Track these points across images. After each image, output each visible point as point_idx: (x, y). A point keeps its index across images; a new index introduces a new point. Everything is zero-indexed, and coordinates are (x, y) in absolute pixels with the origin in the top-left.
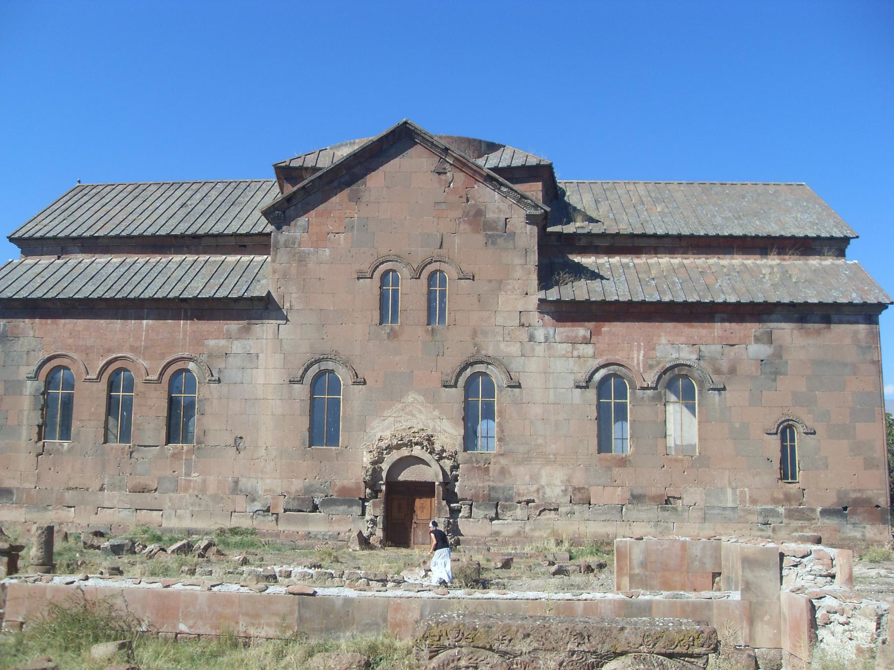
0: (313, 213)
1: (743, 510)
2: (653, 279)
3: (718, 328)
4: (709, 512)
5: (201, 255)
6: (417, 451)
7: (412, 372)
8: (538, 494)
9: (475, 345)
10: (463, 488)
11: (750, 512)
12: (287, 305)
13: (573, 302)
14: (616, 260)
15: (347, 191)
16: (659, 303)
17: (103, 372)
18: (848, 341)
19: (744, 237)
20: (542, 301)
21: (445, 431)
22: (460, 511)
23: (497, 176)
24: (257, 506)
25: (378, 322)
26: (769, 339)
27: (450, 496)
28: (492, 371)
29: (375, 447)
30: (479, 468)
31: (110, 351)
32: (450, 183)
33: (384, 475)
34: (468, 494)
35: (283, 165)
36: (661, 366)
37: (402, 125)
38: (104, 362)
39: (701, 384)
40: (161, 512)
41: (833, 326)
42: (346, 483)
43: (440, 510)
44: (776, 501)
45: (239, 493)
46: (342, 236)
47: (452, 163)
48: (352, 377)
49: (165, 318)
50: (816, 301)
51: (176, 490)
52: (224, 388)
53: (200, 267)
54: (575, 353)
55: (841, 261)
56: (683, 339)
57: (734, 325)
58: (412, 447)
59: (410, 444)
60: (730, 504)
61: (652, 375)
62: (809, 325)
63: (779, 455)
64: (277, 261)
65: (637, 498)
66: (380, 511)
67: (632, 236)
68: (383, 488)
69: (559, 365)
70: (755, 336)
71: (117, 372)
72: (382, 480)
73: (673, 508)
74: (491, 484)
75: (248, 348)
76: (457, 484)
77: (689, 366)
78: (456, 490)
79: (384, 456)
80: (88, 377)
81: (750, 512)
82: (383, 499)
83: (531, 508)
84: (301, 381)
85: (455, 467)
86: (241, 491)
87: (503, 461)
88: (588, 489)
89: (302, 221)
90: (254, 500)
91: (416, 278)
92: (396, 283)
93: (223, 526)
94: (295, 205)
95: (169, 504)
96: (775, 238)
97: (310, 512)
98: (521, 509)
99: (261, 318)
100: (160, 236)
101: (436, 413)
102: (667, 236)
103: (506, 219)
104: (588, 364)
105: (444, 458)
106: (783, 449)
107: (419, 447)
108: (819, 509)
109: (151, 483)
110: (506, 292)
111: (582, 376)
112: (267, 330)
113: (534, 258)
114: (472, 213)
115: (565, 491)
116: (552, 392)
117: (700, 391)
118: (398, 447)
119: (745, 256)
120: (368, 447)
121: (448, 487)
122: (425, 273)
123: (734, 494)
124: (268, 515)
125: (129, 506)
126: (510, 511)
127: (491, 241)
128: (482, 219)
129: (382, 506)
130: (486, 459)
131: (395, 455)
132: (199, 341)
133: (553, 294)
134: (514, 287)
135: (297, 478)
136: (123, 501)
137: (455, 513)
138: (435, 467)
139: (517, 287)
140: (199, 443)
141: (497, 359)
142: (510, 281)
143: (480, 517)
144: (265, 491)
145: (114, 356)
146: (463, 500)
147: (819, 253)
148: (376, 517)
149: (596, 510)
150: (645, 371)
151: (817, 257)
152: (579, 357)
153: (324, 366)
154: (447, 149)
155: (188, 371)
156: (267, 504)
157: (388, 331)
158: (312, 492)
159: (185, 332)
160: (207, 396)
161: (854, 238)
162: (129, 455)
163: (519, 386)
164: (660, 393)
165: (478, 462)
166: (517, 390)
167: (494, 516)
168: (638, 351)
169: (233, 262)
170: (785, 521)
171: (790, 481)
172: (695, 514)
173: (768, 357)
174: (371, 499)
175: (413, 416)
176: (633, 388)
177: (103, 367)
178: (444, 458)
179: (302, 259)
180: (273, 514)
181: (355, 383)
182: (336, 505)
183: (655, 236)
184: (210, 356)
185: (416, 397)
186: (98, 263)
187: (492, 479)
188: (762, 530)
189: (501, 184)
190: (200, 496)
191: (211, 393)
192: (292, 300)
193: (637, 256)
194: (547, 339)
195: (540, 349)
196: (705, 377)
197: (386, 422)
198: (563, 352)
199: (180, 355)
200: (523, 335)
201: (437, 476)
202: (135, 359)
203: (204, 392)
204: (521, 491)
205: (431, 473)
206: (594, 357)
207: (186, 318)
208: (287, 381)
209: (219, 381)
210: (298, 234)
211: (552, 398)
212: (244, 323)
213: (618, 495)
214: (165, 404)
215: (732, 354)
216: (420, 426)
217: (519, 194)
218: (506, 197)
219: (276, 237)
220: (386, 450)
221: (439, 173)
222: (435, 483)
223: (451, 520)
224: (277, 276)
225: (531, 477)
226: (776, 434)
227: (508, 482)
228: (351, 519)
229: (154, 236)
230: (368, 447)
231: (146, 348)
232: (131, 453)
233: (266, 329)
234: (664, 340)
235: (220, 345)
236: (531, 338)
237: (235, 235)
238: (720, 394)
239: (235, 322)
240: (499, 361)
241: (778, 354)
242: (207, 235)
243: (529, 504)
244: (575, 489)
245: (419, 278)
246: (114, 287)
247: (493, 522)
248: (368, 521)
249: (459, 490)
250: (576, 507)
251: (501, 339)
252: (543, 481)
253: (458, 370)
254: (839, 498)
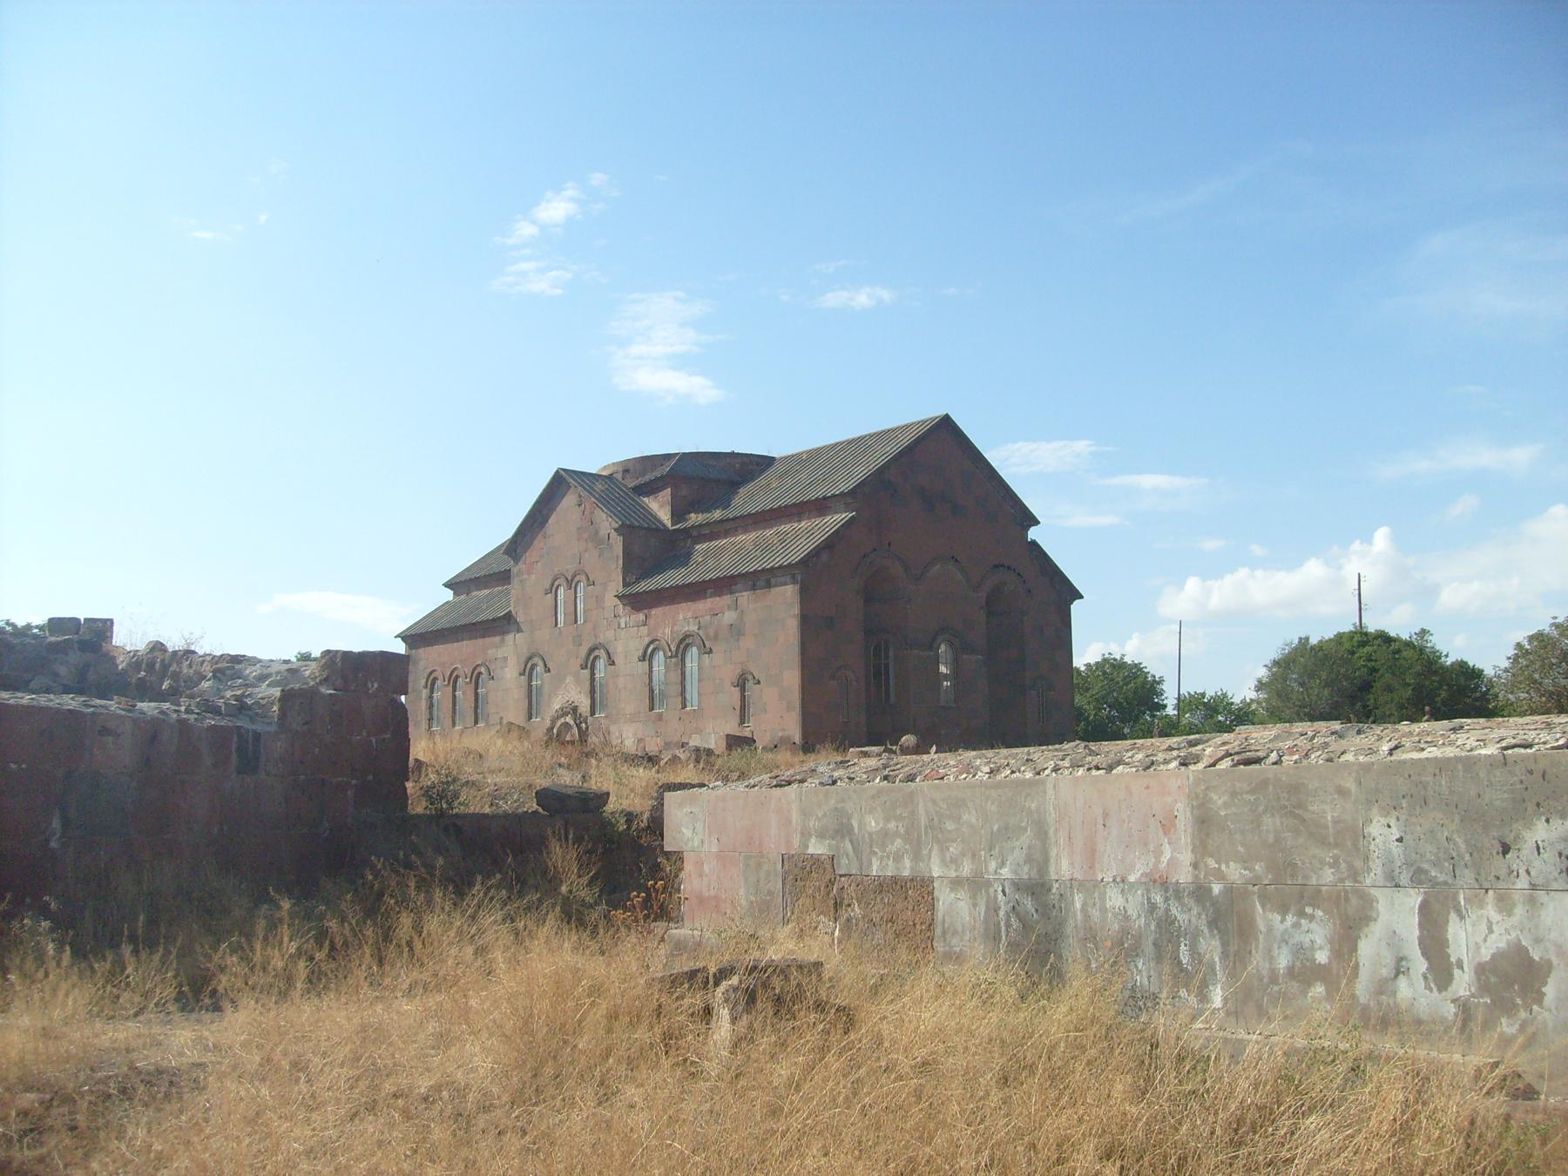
6: (569, 719)
46: (539, 564)
77: (693, 636)
106: (743, 698)
111: (640, 653)
113: (621, 562)
122: (573, 586)
138: (575, 730)
166: (613, 667)
195: (623, 633)
209: (493, 678)
221: (579, 505)
233: (509, 638)
234: (681, 617)
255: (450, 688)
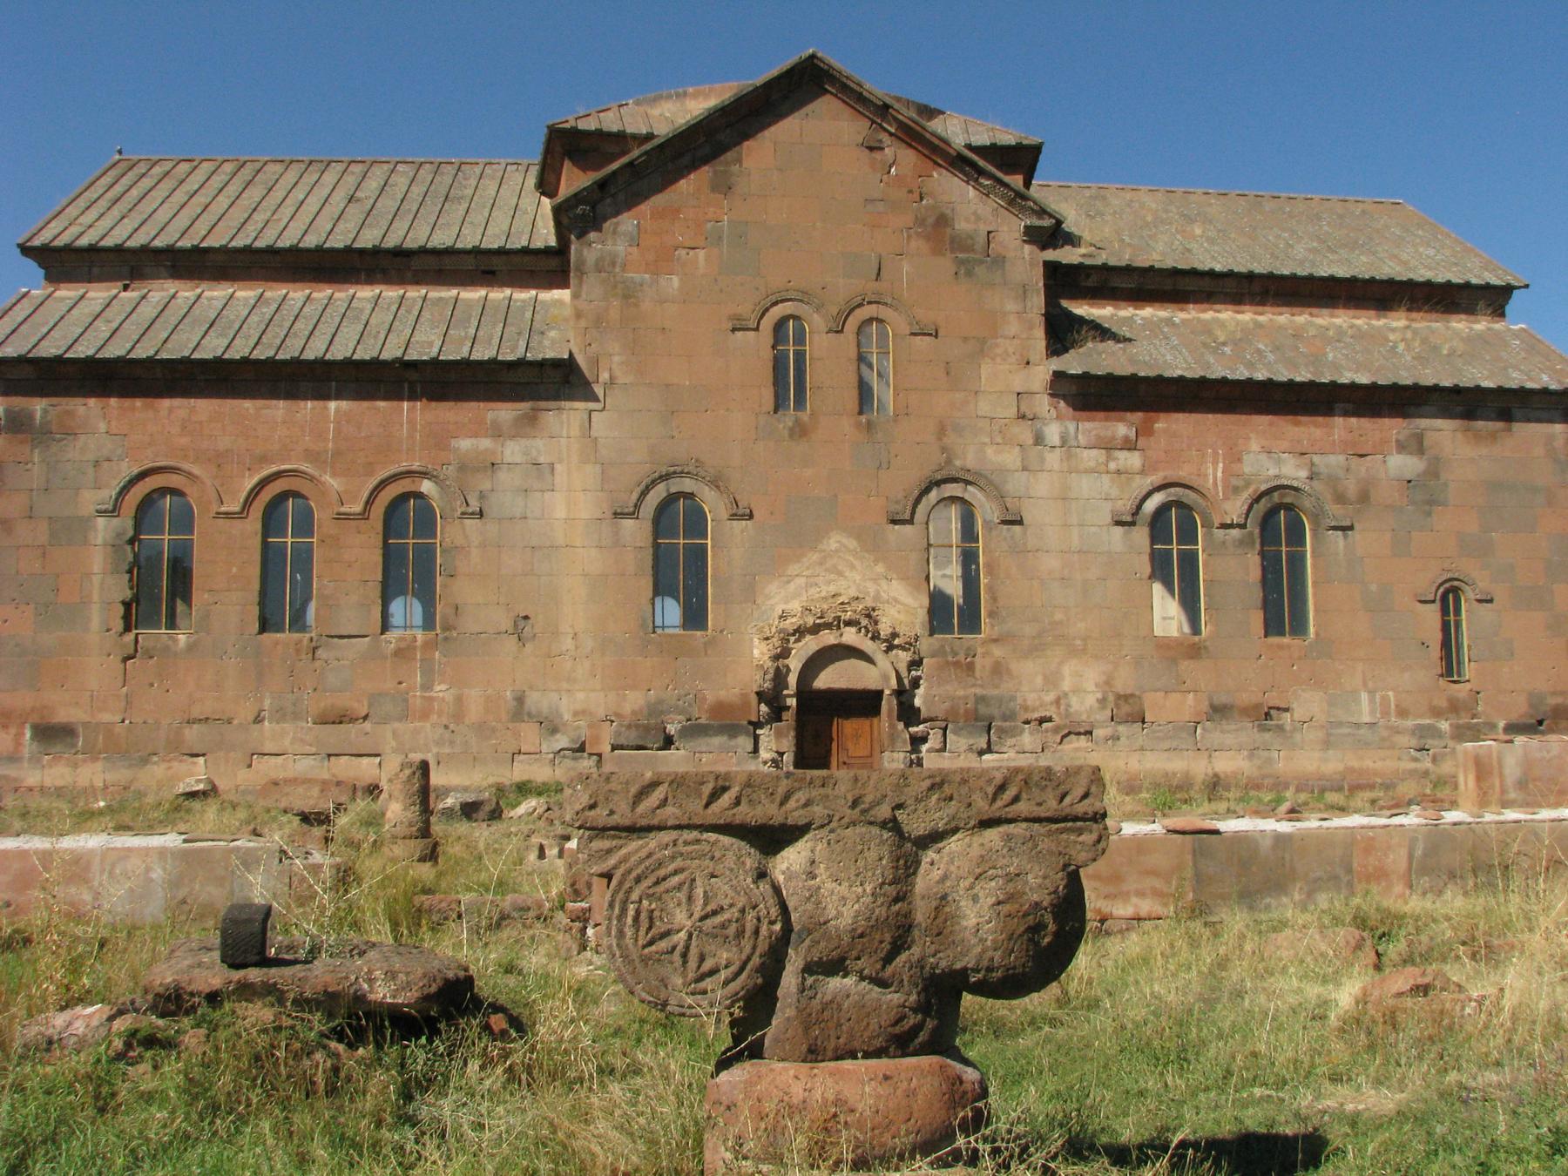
0: (645, 208)
1: (1387, 728)
2: (1224, 344)
3: (1341, 427)
4: (1333, 731)
5: (409, 287)
6: (850, 636)
7: (836, 496)
8: (1059, 708)
9: (944, 450)
10: (928, 699)
11: (1397, 731)
12: (605, 376)
13: (1110, 379)
14: (1147, 311)
15: (705, 172)
16: (1250, 382)
17: (254, 499)
18: (1538, 451)
19: (1353, 281)
20: (1058, 376)
21: (896, 600)
22: (924, 739)
23: (975, 158)
24: (562, 741)
25: (770, 405)
26: (1417, 445)
27: (908, 714)
28: (972, 494)
29: (774, 630)
30: (957, 664)
31: (264, 459)
32: (890, 167)
33: (792, 679)
34: (940, 710)
35: (567, 126)
36: (1251, 490)
37: (807, 59)
38: (256, 479)
39: (1316, 519)
40: (378, 760)
41: (1516, 426)
42: (723, 694)
43: (893, 737)
44: (1437, 713)
45: (526, 718)
46: (701, 254)
47: (893, 131)
48: (729, 506)
49: (371, 396)
50: (1492, 385)
51: (404, 717)
52: (491, 528)
53: (418, 307)
54: (1112, 466)
55: (1499, 326)
56: (1285, 445)
57: (1365, 423)
58: (839, 627)
59: (836, 624)
60: (1366, 719)
61: (1239, 504)
62: (1481, 423)
63: (1439, 636)
64: (584, 296)
65: (1219, 711)
66: (788, 744)
67: (1175, 272)
68: (792, 702)
69: (1085, 486)
70: (1397, 441)
71: (283, 497)
72: (787, 688)
73: (1277, 726)
74: (978, 691)
75: (534, 453)
76: (920, 692)
77: (1296, 489)
78: (917, 702)
79: (791, 645)
80: (223, 509)
81: (1397, 731)
82: (792, 723)
83: (1047, 731)
84: (634, 514)
85: (916, 663)
86: (529, 715)
87: (998, 651)
88: (1140, 698)
89: (627, 222)
90: (554, 731)
91: (837, 332)
92: (800, 338)
93: (500, 780)
94: (613, 196)
95: (394, 744)
96: (1401, 283)
97: (659, 749)
98: (1031, 734)
99: (557, 398)
100: (333, 251)
101: (880, 568)
102: (1230, 274)
103: (989, 232)
104: (1134, 485)
105: (898, 647)
106: (1445, 627)
107: (853, 630)
108: (1502, 724)
109: (356, 705)
110: (993, 359)
111: (1125, 505)
112: (568, 419)
114: (931, 221)
115: (1102, 701)
116: (1075, 532)
117: (1314, 531)
118: (815, 630)
119: (1352, 312)
120: (761, 630)
121: (903, 699)
123: (1372, 701)
124: (581, 757)
125: (314, 750)
126: (1012, 737)
127: (965, 269)
128: (949, 230)
129: (792, 733)
130: (969, 649)
131: (810, 645)
132: (440, 440)
133: (1074, 362)
134: (1006, 351)
135: (633, 687)
136: (302, 740)
137: (918, 741)
139: (1011, 350)
140: (446, 628)
141: (981, 475)
142: (999, 340)
143: (962, 750)
144: (576, 714)
145: (274, 469)
146: (931, 720)
147: (1470, 310)
148: (781, 754)
149: (1154, 732)
150: (1226, 498)
151: (1463, 316)
152: (1118, 472)
153: (676, 486)
154: (886, 107)
155: (419, 496)
156: (579, 737)
157: (790, 424)
158: (662, 712)
159: (411, 422)
160: (460, 541)
161: (1520, 287)
162: (310, 655)
163: (1020, 522)
164: (1251, 534)
165: (955, 654)
166: (1017, 528)
167: (985, 746)
168: (1215, 463)
169: (478, 300)
170: (1451, 744)
171: (1455, 678)
172: (1312, 735)
173: (1419, 475)
174: (767, 722)
175: (841, 574)
176: (1207, 525)
177: (252, 490)
178: (898, 647)
179: (629, 295)
180: (591, 754)
181: (734, 516)
182: (707, 735)
183: (1211, 274)
184: (462, 468)
185: (845, 541)
186: (210, 299)
187: (979, 682)
188: (1416, 760)
189: (981, 172)
190: (452, 726)
191: (466, 537)
192: (614, 366)
193: (1181, 306)
194: (1064, 441)
195: (1053, 459)
196: (1322, 508)
197: (792, 586)
198: (1092, 464)
199: (404, 466)
200: (1024, 433)
201: (886, 678)
202: (316, 473)
203: (448, 533)
204: (1029, 703)
205: (877, 674)
206: (1143, 472)
207: (413, 397)
208: (609, 514)
209: (481, 514)
210: (620, 248)
211: (1075, 543)
212: (525, 406)
213: (1189, 705)
214: (377, 557)
215: (1363, 469)
216: (853, 592)
217: (1012, 189)
218: (987, 195)
219: (579, 252)
220: (793, 635)
221: (871, 149)
222: (879, 693)
223: (913, 756)
224: (583, 323)
225: (1045, 678)
226: (1433, 602)
227: (1006, 687)
228: (734, 760)
229: (319, 251)
230: (761, 630)
231: (337, 453)
232: (314, 649)
233: (566, 418)
234: (1254, 446)
235: (482, 447)
236: (1039, 440)
237: (477, 252)
238: (1345, 537)
239: (509, 405)
240: (986, 478)
241: (1433, 472)
242: (423, 251)
243: (1045, 725)
244: (1119, 697)
245: (841, 331)
246: (264, 339)
247: (984, 757)
248: (765, 763)
249: (924, 702)
250: (1122, 729)
251: (987, 440)
252: (1066, 685)
253: (916, 492)
254: (1531, 706)
255: (254, 523)
